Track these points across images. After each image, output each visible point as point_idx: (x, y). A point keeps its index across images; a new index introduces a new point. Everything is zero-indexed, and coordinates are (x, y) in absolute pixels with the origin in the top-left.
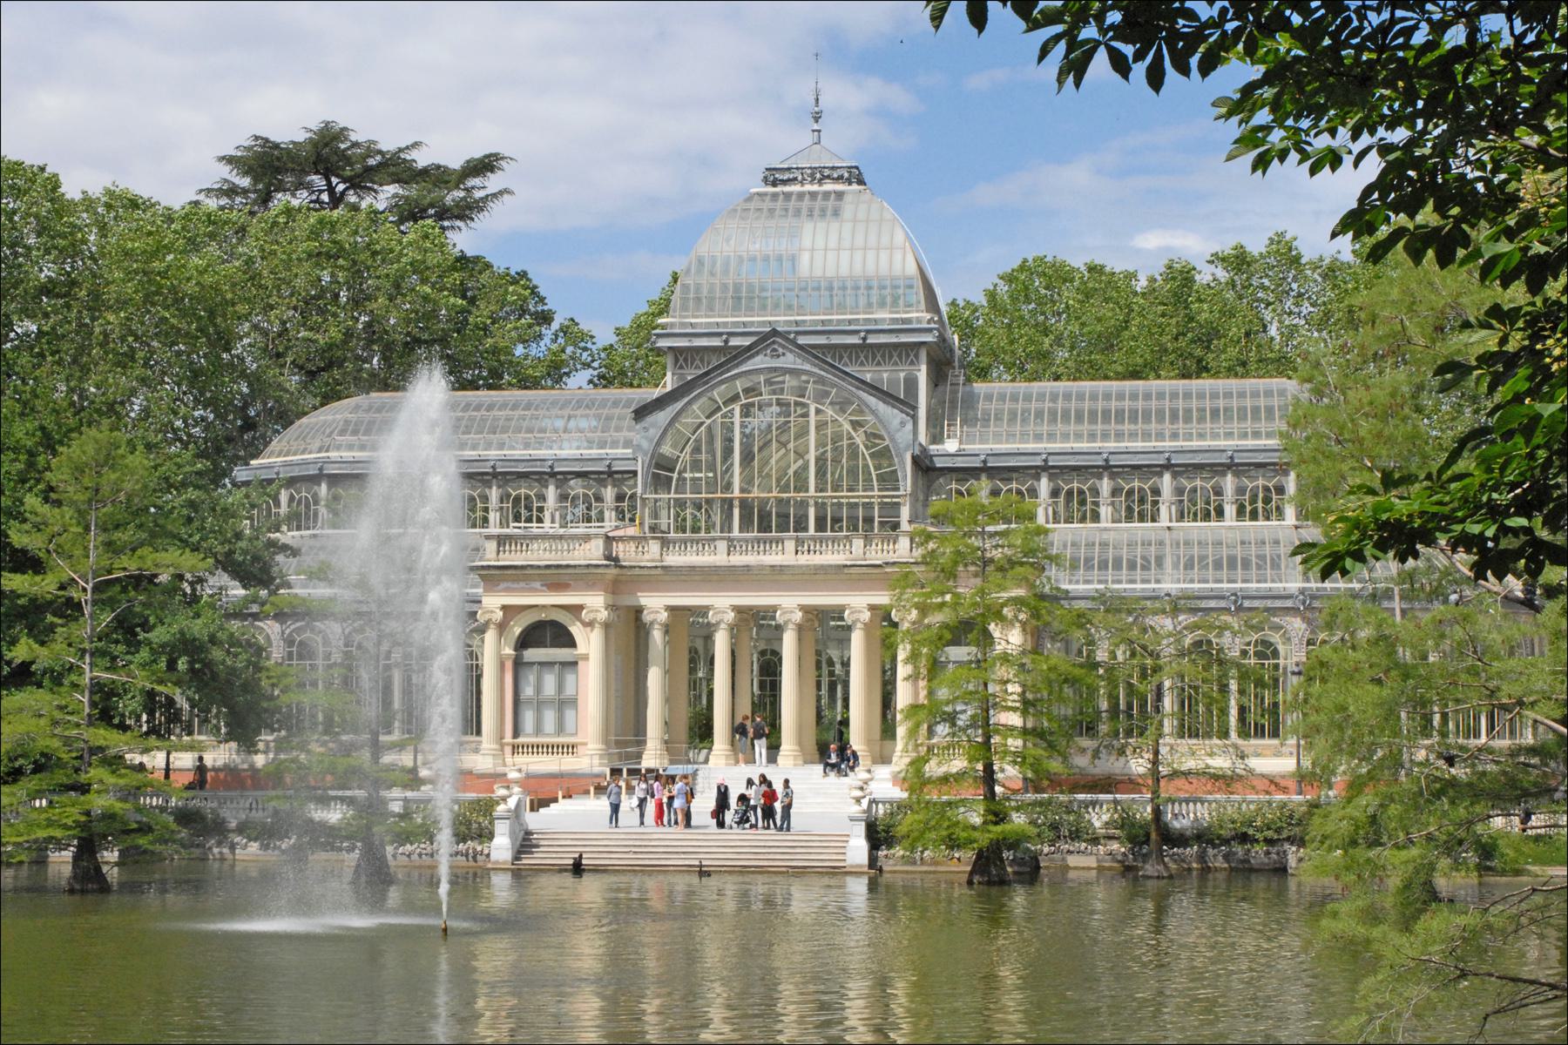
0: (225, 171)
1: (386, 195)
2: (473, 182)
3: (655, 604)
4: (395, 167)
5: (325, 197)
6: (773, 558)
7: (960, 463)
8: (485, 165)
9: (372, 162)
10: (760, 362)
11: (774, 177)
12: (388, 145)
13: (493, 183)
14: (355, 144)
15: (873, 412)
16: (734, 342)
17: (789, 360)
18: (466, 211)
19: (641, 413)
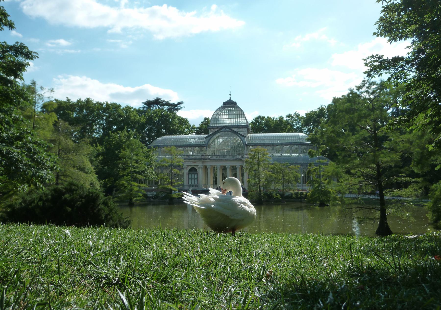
0: (143, 105)
1: (166, 108)
2: (179, 106)
4: (167, 104)
8: (180, 103)
9: (164, 103)
11: (224, 104)
12: (166, 100)
13: (181, 106)
14: (161, 100)
16: (219, 127)
17: (227, 130)
18: (177, 109)
19: (206, 138)
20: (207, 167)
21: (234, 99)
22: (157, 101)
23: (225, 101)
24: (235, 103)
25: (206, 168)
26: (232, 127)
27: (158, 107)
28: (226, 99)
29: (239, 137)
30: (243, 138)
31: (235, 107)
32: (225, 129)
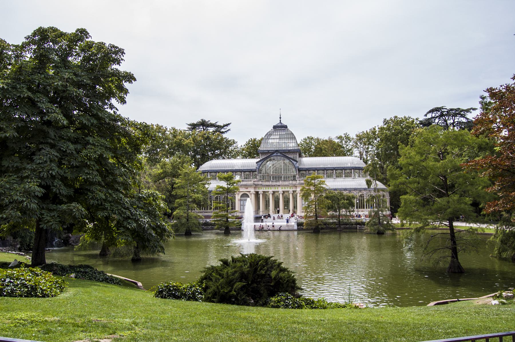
1: (211, 130)
2: (225, 128)
3: (261, 191)
4: (212, 125)
5: (202, 130)
6: (278, 183)
7: (304, 169)
10: (275, 154)
11: (275, 127)
12: (213, 122)
13: (228, 128)
15: (292, 162)
16: (270, 151)
17: (279, 154)
18: (223, 133)
19: (257, 163)
20: (259, 193)
21: (284, 123)
22: (204, 124)
23: (275, 125)
24: (286, 127)
25: (257, 194)
26: (283, 151)
27: (203, 129)
28: (276, 122)
29: (292, 162)
30: (295, 163)
31: (286, 130)
32: (277, 154)
